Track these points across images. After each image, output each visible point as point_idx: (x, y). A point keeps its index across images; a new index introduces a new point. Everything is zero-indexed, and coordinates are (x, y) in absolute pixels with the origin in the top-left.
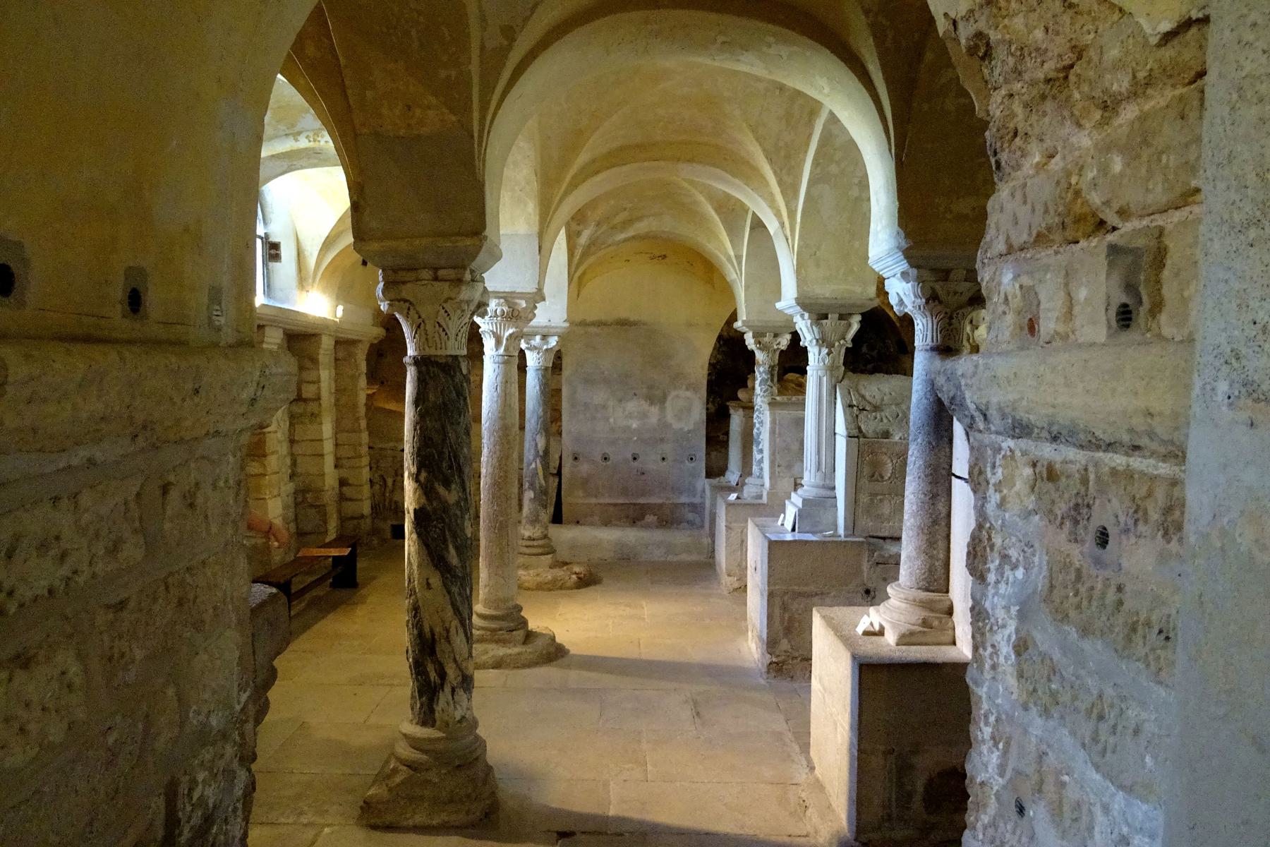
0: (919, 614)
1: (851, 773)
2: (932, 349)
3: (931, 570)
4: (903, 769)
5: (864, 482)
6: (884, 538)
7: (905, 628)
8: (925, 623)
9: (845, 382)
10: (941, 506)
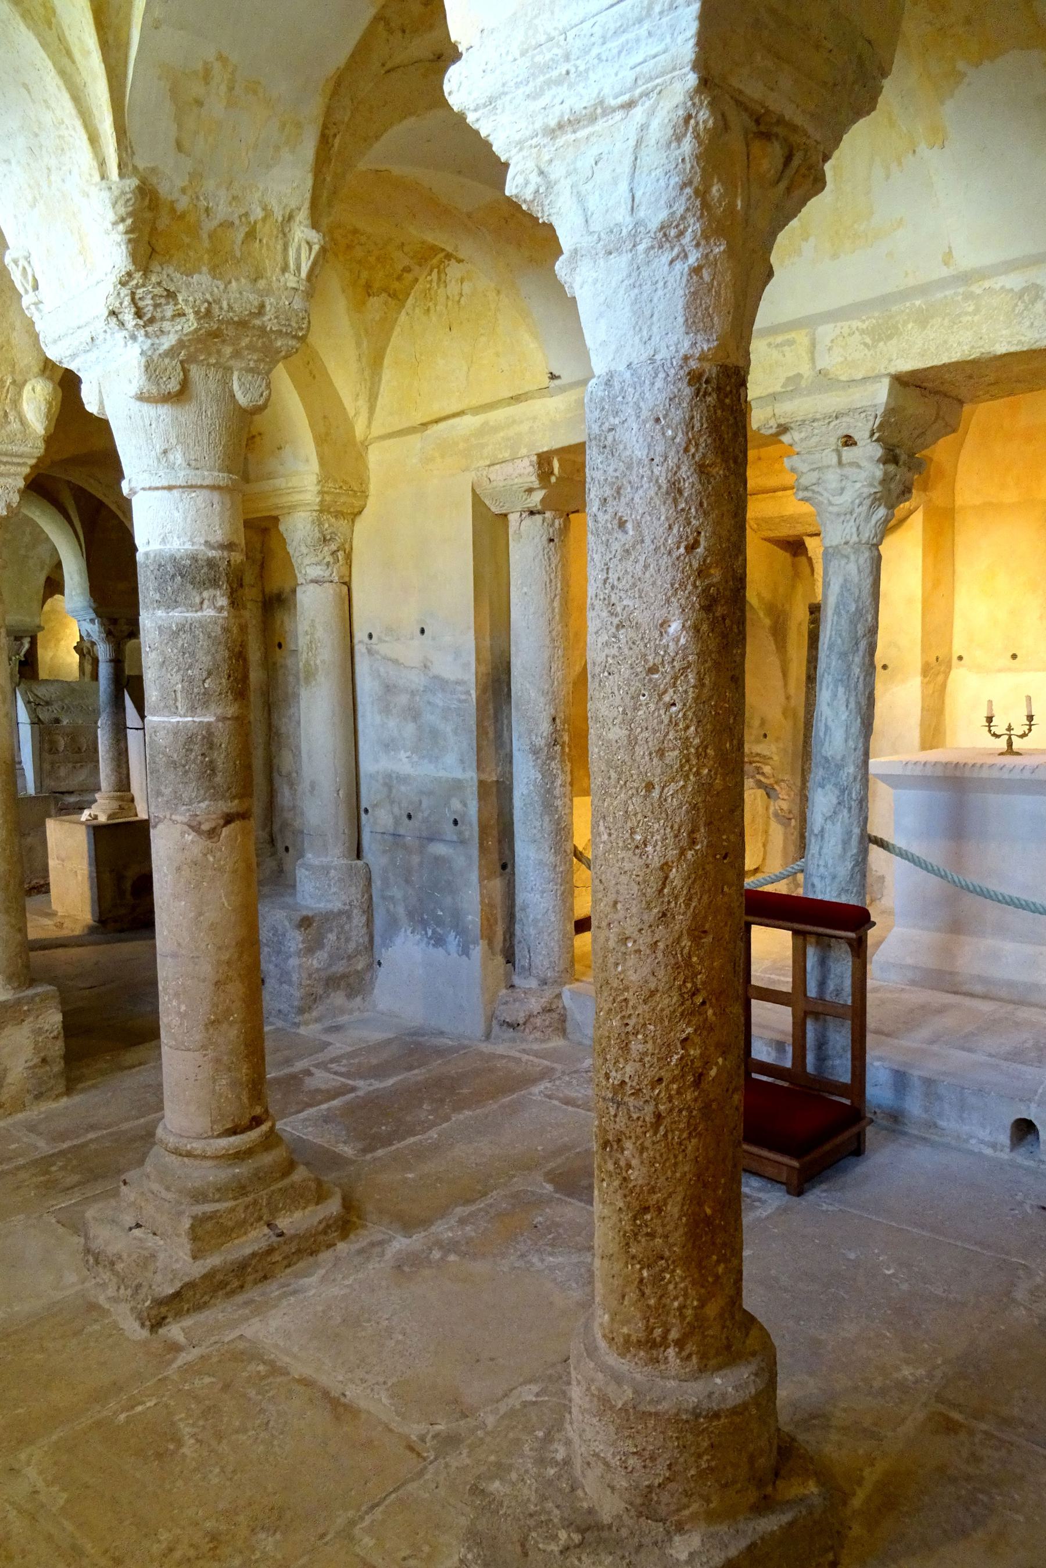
0: (115, 805)
1: (91, 888)
2: (111, 661)
3: (121, 781)
4: (120, 878)
5: (46, 755)
6: (62, 793)
7: (110, 812)
8: (121, 808)
9: (22, 685)
10: (122, 745)
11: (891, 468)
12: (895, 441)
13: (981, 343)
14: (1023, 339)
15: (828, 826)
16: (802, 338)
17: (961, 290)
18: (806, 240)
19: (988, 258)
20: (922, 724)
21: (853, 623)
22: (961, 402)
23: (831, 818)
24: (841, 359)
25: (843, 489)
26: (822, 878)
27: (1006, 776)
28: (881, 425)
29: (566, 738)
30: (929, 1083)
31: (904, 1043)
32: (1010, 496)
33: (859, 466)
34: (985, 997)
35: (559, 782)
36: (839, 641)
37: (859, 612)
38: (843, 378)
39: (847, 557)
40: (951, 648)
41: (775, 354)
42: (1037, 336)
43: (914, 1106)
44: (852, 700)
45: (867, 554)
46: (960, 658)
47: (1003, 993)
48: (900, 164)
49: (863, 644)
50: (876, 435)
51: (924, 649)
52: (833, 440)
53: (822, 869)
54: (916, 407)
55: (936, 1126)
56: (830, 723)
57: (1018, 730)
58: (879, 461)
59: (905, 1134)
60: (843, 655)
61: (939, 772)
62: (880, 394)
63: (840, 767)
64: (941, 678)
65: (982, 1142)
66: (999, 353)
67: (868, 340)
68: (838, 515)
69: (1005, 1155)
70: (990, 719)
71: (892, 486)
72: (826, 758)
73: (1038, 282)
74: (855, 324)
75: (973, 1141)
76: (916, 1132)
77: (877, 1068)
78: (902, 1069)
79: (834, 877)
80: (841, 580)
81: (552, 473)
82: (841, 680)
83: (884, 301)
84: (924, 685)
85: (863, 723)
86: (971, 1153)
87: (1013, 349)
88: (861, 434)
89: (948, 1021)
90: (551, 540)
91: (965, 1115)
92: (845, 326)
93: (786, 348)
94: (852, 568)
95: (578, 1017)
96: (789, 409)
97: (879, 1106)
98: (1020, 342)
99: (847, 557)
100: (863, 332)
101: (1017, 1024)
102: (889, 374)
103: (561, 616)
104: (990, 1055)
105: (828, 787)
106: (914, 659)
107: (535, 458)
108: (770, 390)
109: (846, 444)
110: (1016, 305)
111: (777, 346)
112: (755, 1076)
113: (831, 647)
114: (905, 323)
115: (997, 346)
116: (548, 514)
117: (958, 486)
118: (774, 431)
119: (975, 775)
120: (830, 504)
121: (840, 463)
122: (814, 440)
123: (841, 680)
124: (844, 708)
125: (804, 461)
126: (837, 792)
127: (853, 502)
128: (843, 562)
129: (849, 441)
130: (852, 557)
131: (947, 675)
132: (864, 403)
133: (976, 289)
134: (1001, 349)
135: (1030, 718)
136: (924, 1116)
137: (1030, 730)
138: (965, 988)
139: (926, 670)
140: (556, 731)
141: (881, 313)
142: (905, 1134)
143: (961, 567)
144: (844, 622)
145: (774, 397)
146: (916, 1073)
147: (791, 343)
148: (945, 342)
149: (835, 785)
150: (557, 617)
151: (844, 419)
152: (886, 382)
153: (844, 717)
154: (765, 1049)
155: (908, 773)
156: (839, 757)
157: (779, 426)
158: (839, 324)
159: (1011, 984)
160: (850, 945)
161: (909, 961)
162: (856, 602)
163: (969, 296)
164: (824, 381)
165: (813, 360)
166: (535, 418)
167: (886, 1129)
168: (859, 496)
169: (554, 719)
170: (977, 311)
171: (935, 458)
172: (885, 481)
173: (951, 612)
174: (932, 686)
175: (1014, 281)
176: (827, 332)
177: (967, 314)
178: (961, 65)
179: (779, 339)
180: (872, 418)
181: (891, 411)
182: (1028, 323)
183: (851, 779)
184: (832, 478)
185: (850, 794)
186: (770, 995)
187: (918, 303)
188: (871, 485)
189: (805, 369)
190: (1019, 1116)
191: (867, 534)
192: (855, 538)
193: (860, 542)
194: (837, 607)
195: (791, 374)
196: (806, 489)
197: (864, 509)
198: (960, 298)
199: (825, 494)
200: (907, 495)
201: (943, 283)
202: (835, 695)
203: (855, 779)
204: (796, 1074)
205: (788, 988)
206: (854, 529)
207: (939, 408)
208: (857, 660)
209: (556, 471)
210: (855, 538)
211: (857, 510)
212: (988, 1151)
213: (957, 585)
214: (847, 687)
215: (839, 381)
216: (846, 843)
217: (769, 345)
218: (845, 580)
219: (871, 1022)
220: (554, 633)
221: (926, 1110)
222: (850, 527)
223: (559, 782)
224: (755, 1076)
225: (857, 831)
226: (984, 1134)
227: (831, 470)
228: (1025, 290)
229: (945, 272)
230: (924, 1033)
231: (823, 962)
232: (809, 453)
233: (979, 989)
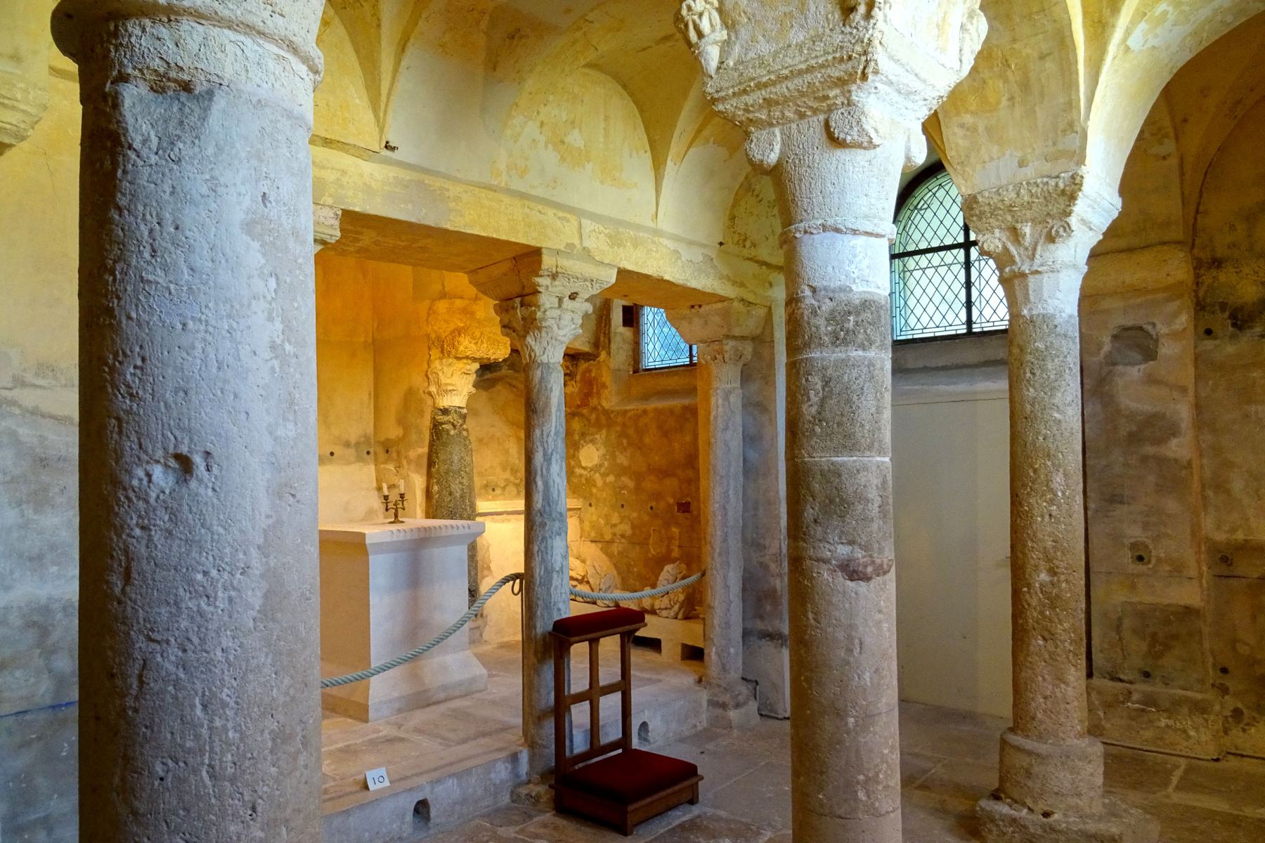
47: (457, 693)
62: (611, 277)
83: (620, 223)
107: (340, 213)
113: (556, 434)
134: (667, 277)
138: (434, 699)
141: (618, 229)
145: (558, 252)
147: (568, 221)
155: (395, 539)
161: (396, 694)
163: (654, 242)
164: (587, 255)
166: (344, 172)
176: (588, 225)
179: (561, 214)
189: (577, 242)
229: (652, 225)
233: (442, 695)
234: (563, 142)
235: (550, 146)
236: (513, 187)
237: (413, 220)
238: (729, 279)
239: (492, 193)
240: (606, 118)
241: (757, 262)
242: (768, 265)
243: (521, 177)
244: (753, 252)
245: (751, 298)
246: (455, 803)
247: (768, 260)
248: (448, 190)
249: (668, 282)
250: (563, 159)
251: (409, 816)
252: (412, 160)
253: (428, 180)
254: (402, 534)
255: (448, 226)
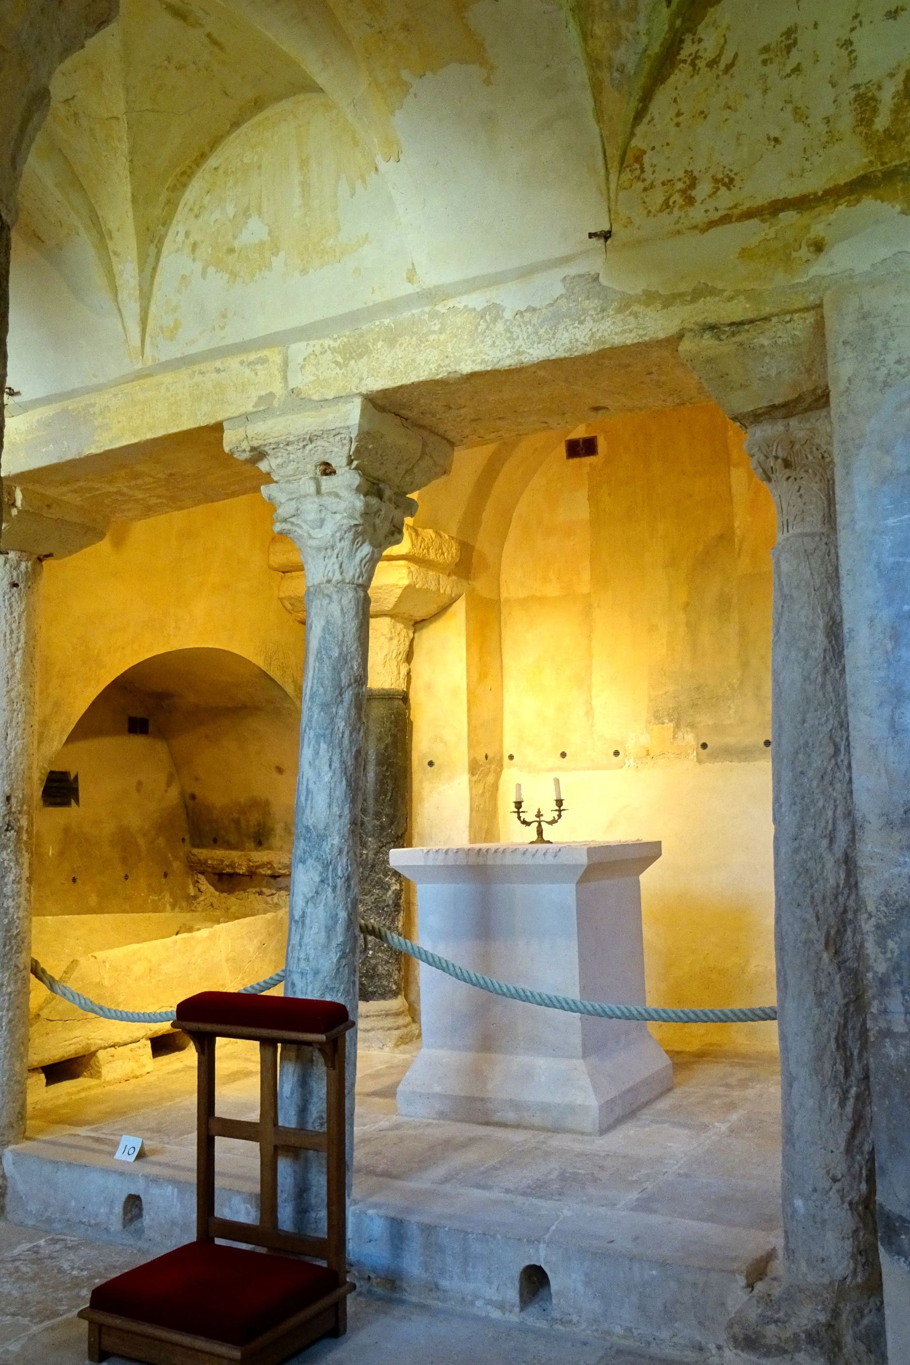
11: (374, 501)
12: (380, 474)
13: (447, 362)
14: (487, 358)
15: (309, 911)
16: (274, 356)
17: (427, 309)
18: (276, 254)
19: (450, 275)
20: (470, 826)
21: (336, 671)
22: (452, 444)
23: (311, 900)
24: (312, 378)
25: (322, 522)
26: (303, 974)
27: (529, 861)
28: (357, 450)
29: (24, 822)
30: (428, 1230)
31: (411, 1185)
32: (552, 590)
33: (337, 496)
34: (517, 1126)
35: (11, 877)
36: (321, 690)
37: (343, 659)
38: (315, 397)
39: (330, 597)
40: (501, 746)
41: (248, 372)
42: (499, 355)
43: (413, 1266)
44: (336, 758)
45: (351, 594)
46: (511, 757)
47: (537, 1120)
48: (364, 182)
49: (348, 696)
50: (355, 463)
51: (470, 746)
52: (310, 467)
53: (303, 964)
54: (393, 435)
55: (437, 1287)
56: (311, 786)
57: (548, 816)
58: (358, 490)
59: (402, 1302)
60: (325, 706)
61: (462, 861)
62: (352, 415)
63: (322, 838)
64: (491, 779)
65: (489, 1302)
66: (465, 372)
67: (340, 359)
68: (319, 549)
69: (514, 1317)
70: (518, 805)
71: (378, 521)
72: (307, 827)
73: (498, 302)
74: (327, 342)
75: (479, 1303)
76: (414, 1299)
77: (371, 1219)
78: (399, 1216)
79: (316, 973)
80: (323, 623)
81: (13, 505)
82: (324, 735)
83: (353, 318)
84: (472, 785)
85: (349, 784)
86: (476, 1318)
87: (477, 368)
88: (338, 461)
89: (471, 1156)
90: (15, 585)
91: (469, 1269)
92: (316, 345)
93: (259, 367)
94: (335, 609)
95: (21, 1188)
96: (264, 430)
97: (374, 1270)
98: (483, 361)
99: (330, 597)
100: (334, 350)
101: (547, 1154)
102: (360, 394)
103: (25, 674)
104: (507, 1191)
105: (310, 862)
106: (461, 756)
108: (242, 410)
109: (325, 473)
110: (479, 324)
111: (250, 364)
112: (219, 1241)
113: (312, 697)
114: (374, 344)
115: (462, 364)
116: (12, 555)
117: (503, 577)
118: (247, 455)
119: (499, 863)
120: (310, 537)
121: (318, 492)
122: (292, 466)
123: (324, 735)
124: (326, 768)
125: (281, 490)
126: (320, 868)
127: (333, 536)
128: (326, 601)
129: (327, 469)
130: (335, 597)
131: (498, 774)
132: (338, 425)
133: (441, 308)
134: (466, 368)
135: (559, 802)
136: (424, 1276)
137: (560, 816)
138: (497, 1117)
139: (474, 767)
140: (10, 813)
141: (352, 329)
142: (402, 1302)
143: (507, 661)
144: (327, 670)
145: (247, 417)
146: (414, 1218)
147: (263, 361)
148: (413, 360)
149: (318, 859)
150: (18, 675)
151: (320, 442)
152: (358, 402)
153: (327, 779)
154: (243, 1207)
155: (430, 863)
156: (321, 826)
157: (253, 449)
158: (311, 343)
159: (545, 1108)
160: (322, 1051)
161: (437, 1089)
162: (341, 646)
163: (434, 315)
164: (297, 400)
165: (285, 379)
167: (381, 1299)
168: (339, 529)
169: (8, 798)
170: (441, 331)
171: (478, 547)
172: (366, 514)
173: (501, 708)
174: (481, 785)
175: (476, 300)
176: (299, 350)
177: (434, 332)
178: (405, 75)
179: (253, 356)
180: (346, 442)
181: (365, 435)
182: (490, 342)
183: (336, 851)
184: (310, 508)
185: (335, 869)
186: (236, 1129)
187: (386, 322)
188: (352, 517)
189: (277, 388)
190: (527, 1263)
191: (352, 571)
192: (337, 577)
193: (343, 581)
194: (319, 652)
195: (263, 393)
196: (285, 520)
197: (346, 543)
198: (426, 317)
199: (305, 527)
200: (397, 536)
201: (408, 301)
202: (317, 753)
203: (340, 852)
204: (265, 1230)
205: (254, 1116)
206: (337, 566)
207: (425, 444)
208: (341, 712)
209: (19, 503)
210: (337, 577)
211: (339, 545)
212: (495, 1314)
213: (505, 681)
214: (330, 744)
215: (311, 400)
216: (330, 930)
217: (242, 363)
218: (328, 622)
219: (359, 1156)
220: (13, 694)
221: (426, 1266)
222: (332, 564)
223: (11, 877)
224: (219, 1241)
225: (343, 915)
226: (491, 1293)
227: (309, 499)
228: (486, 310)
229: (409, 289)
230: (440, 1171)
231: (304, 1083)
232: (288, 482)
234: (231, 251)
235: (211, 270)
236: (163, 359)
237: (54, 461)
238: (649, 298)
239: (149, 380)
240: (304, 163)
241: (749, 215)
242: (802, 203)
243: (172, 339)
244: (726, 200)
245: (739, 310)
246: (174, 1223)
247: (792, 190)
248: (94, 405)
249: (473, 375)
250: (234, 275)
251: (118, 1209)
252: (41, 393)
253: (71, 404)
254: (441, 857)
255: (94, 450)
